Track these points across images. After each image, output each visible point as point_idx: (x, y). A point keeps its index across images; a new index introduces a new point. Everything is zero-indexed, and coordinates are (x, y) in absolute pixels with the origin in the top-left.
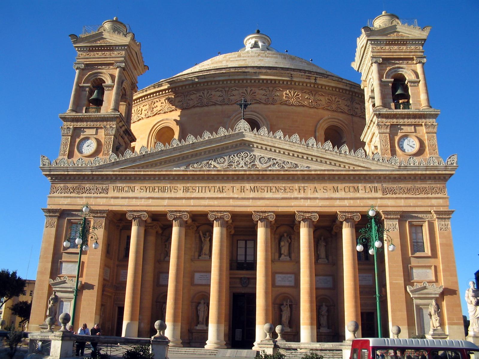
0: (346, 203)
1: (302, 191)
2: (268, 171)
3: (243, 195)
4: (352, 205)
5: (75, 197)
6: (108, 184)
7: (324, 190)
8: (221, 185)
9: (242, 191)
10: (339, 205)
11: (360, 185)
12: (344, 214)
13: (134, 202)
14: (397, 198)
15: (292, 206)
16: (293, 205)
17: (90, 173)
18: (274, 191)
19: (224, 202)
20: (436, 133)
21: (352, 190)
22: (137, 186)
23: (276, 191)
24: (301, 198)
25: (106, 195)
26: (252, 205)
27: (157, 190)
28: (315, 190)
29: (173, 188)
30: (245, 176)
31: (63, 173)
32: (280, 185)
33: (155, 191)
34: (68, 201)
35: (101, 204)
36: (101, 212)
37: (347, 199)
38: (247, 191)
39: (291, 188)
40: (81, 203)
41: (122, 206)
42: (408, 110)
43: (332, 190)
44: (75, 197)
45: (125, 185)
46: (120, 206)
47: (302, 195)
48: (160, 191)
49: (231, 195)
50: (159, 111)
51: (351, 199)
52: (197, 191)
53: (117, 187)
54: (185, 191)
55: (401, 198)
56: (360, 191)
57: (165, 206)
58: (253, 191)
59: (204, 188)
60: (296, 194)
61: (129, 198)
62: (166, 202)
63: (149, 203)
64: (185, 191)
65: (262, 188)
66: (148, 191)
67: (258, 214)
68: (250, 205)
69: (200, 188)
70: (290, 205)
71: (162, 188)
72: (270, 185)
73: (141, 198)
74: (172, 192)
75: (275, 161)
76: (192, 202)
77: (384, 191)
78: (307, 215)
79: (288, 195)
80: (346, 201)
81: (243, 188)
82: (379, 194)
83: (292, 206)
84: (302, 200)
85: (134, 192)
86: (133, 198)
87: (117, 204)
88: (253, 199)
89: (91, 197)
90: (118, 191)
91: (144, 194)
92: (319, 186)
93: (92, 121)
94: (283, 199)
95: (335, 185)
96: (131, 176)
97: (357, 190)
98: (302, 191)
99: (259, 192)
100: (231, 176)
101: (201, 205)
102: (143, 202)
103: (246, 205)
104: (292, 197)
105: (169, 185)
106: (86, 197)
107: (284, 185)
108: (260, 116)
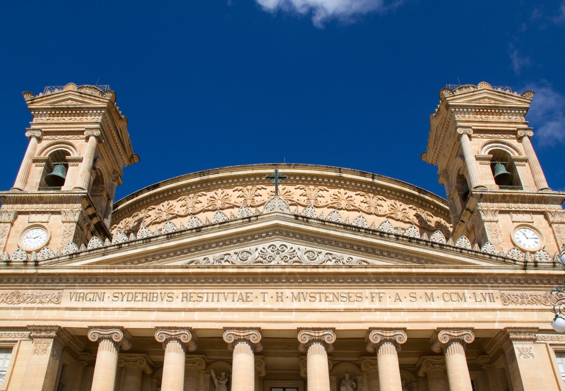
0: (448, 316)
1: (376, 300)
2: (321, 268)
3: (281, 305)
4: (457, 320)
5: (7, 309)
6: (63, 289)
7: (412, 299)
8: (244, 291)
9: (280, 299)
10: (438, 320)
11: (466, 291)
12: (448, 333)
13: (102, 315)
14: (525, 310)
15: (361, 322)
16: (363, 320)
18: (331, 299)
21: (455, 297)
22: (109, 293)
23: (335, 299)
24: (376, 310)
26: (297, 320)
27: (139, 298)
28: (397, 298)
29: (166, 295)
30: (284, 276)
32: (340, 291)
33: (137, 299)
35: (49, 318)
36: (47, 329)
37: (449, 310)
38: (289, 300)
39: (358, 296)
40: (17, 318)
41: (82, 321)
42: (520, 191)
43: (424, 298)
44: (7, 309)
45: (88, 291)
46: (79, 321)
47: (377, 305)
48: (144, 299)
49: (261, 305)
50: (154, 220)
51: (455, 310)
52: (205, 299)
53: (75, 294)
54: (185, 299)
57: (153, 321)
58: (298, 300)
59: (216, 296)
60: (366, 304)
61: (94, 309)
64: (185, 299)
65: (312, 295)
66: (125, 299)
67: (308, 333)
68: (293, 320)
69: (210, 295)
70: (359, 320)
71: (149, 294)
72: (325, 291)
73: (114, 309)
74: (165, 300)
75: (330, 257)
76: (197, 316)
77: (505, 300)
78: (388, 334)
79: (355, 305)
80: (447, 313)
81: (280, 295)
82: (498, 304)
83: (361, 322)
84: (378, 313)
85: (103, 300)
86: (100, 309)
87: (73, 319)
88: (297, 310)
89: (33, 309)
90: (77, 300)
91: (119, 304)
92: (404, 292)
95: (429, 291)
96: (99, 277)
97: (462, 298)
98: (376, 300)
99: (307, 301)
100: (260, 276)
101: (212, 319)
102: (117, 315)
103: (286, 320)
104: (362, 307)
105: (159, 291)
106: (25, 309)
107: (346, 291)
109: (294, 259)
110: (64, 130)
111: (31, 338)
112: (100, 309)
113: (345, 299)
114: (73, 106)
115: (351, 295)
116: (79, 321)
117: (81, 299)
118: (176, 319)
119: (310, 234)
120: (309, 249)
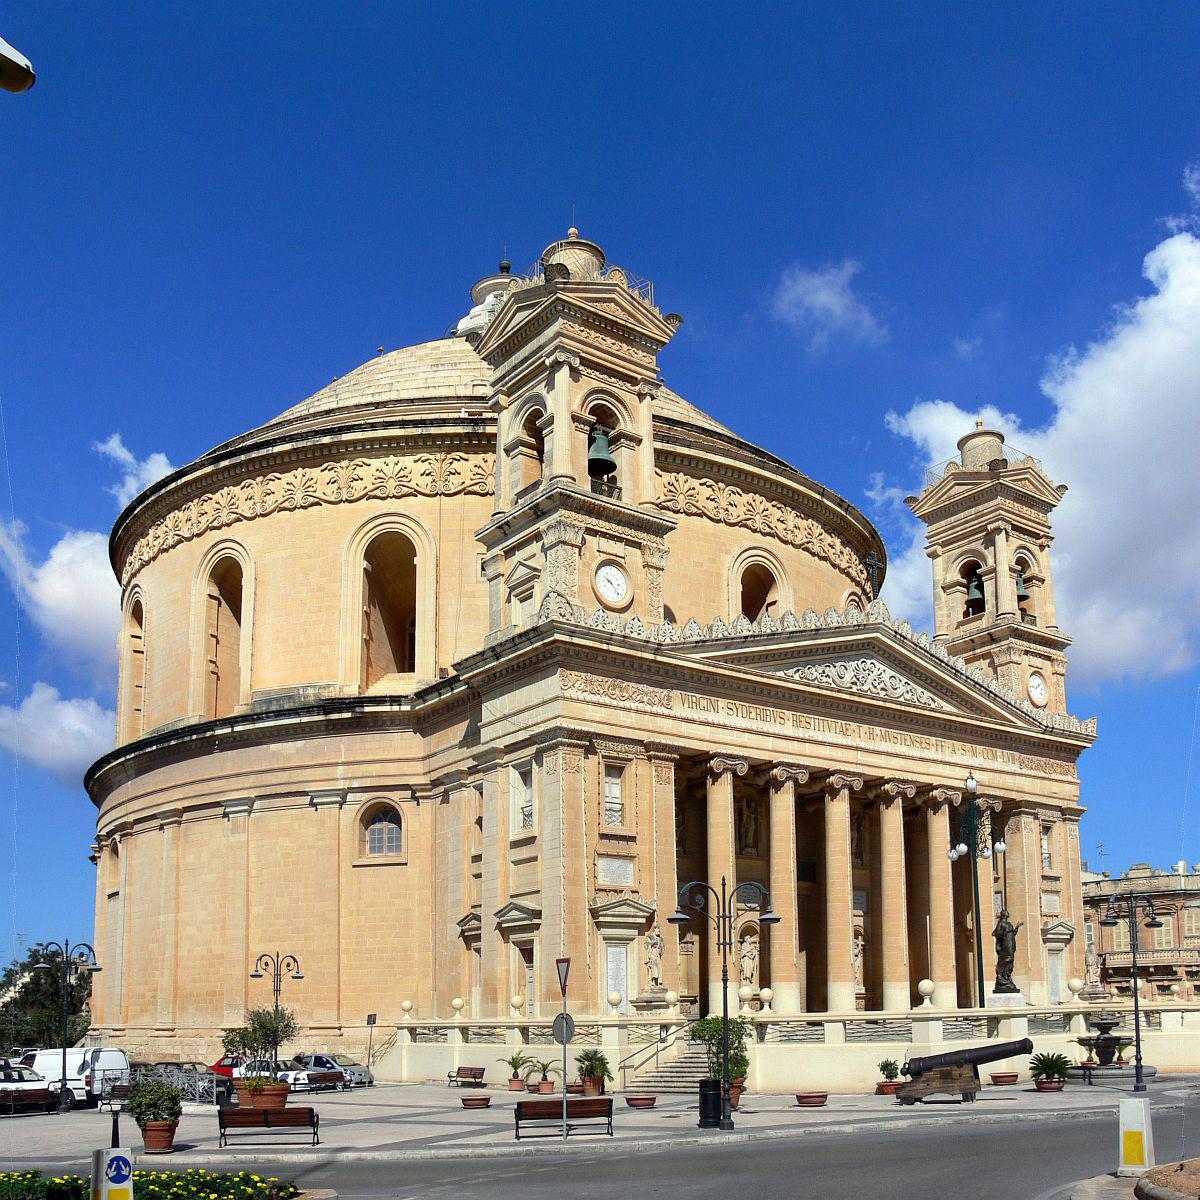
5: (615, 707)
13: (720, 735)
16: (931, 773)
17: (651, 656)
19: (850, 755)
20: (1063, 675)
21: (990, 756)
25: (666, 712)
31: (597, 645)
34: (601, 714)
38: (877, 739)
44: (615, 707)
46: (697, 739)
48: (759, 718)
51: (992, 771)
52: (812, 727)
55: (1038, 777)
56: (999, 759)
61: (713, 725)
62: (770, 743)
63: (743, 739)
66: (740, 715)
76: (808, 748)
86: (718, 726)
89: (645, 712)
93: (619, 523)
94: (922, 759)
106: (637, 711)
108: (774, 561)
109: (882, 685)
110: (609, 365)
111: (650, 758)
112: (718, 726)
113: (918, 745)
114: (624, 323)
115: (923, 740)
116: (697, 739)
117: (694, 705)
118: (790, 751)
119: (897, 655)
120: (894, 674)
